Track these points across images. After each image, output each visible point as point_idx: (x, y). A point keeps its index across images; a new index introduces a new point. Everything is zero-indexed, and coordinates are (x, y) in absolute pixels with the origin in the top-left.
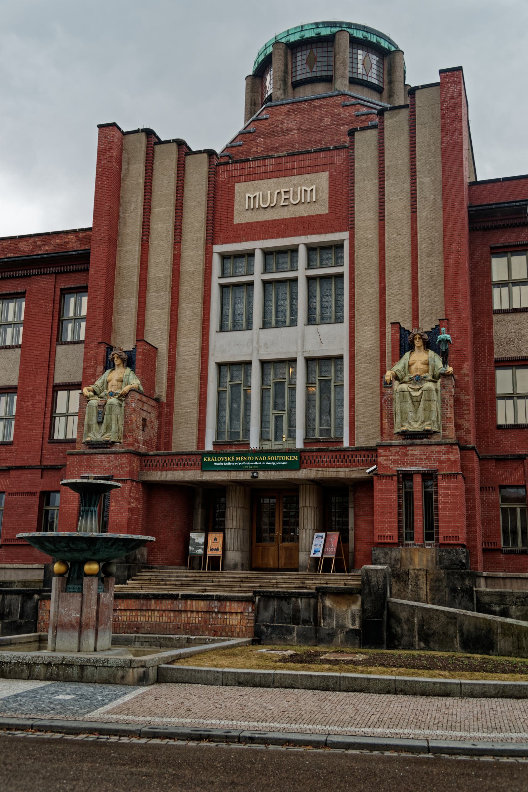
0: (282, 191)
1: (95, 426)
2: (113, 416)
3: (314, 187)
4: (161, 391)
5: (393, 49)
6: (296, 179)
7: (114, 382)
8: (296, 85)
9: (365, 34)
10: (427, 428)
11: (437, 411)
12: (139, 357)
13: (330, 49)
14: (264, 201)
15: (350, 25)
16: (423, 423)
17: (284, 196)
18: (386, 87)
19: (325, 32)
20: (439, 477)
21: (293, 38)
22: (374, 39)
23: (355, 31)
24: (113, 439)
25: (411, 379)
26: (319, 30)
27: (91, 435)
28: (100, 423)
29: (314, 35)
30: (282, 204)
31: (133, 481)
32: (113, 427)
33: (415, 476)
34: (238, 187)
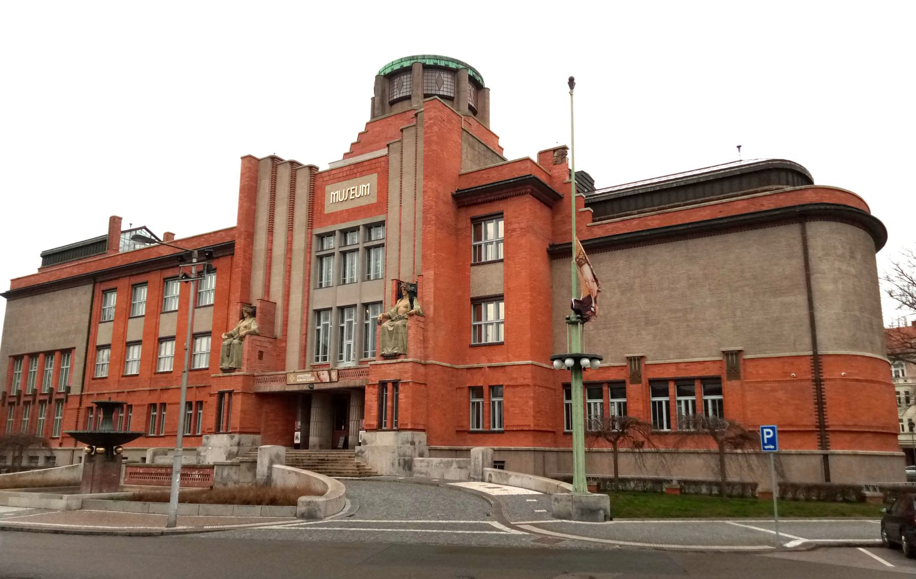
0: (351, 188)
1: (226, 358)
2: (235, 351)
3: (369, 185)
4: (278, 332)
5: (461, 67)
6: (359, 179)
7: (242, 328)
8: (392, 103)
9: (436, 61)
10: (396, 352)
11: (403, 340)
12: (258, 311)
13: (409, 76)
14: (341, 198)
15: (424, 57)
16: (393, 349)
17: (352, 193)
18: (456, 96)
19: (406, 64)
20: (400, 385)
21: (388, 71)
22: (442, 64)
23: (427, 60)
24: (234, 367)
25: (396, 318)
26: (402, 64)
27: (224, 364)
28: (228, 356)
29: (399, 67)
30: (351, 198)
31: (244, 393)
32: (234, 360)
33: (388, 384)
34: (328, 188)
